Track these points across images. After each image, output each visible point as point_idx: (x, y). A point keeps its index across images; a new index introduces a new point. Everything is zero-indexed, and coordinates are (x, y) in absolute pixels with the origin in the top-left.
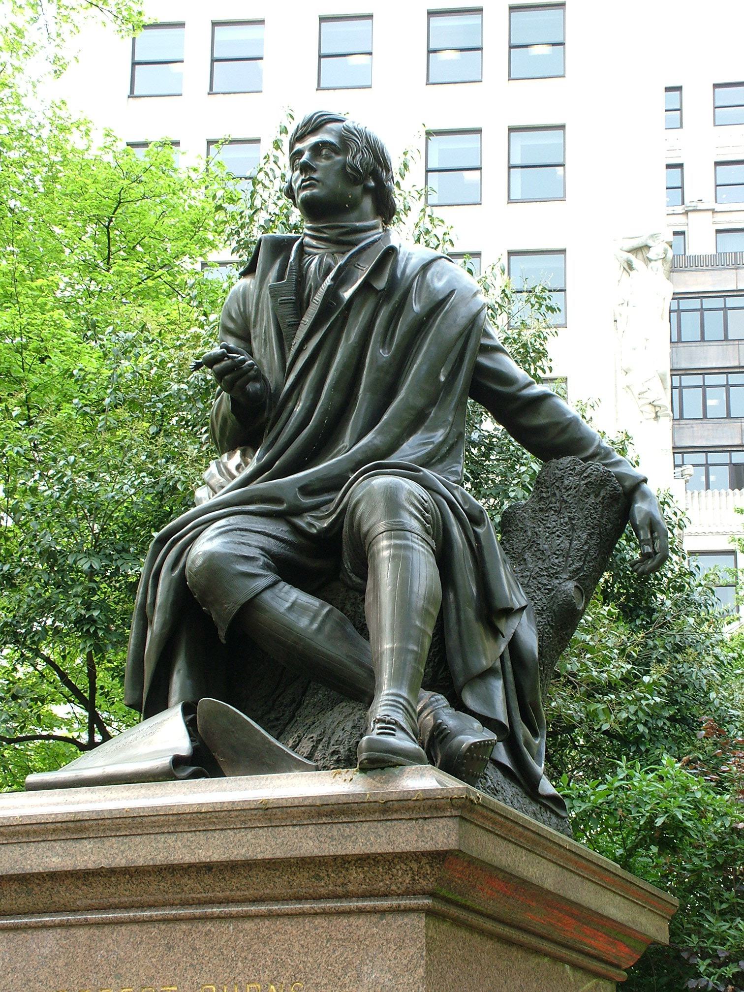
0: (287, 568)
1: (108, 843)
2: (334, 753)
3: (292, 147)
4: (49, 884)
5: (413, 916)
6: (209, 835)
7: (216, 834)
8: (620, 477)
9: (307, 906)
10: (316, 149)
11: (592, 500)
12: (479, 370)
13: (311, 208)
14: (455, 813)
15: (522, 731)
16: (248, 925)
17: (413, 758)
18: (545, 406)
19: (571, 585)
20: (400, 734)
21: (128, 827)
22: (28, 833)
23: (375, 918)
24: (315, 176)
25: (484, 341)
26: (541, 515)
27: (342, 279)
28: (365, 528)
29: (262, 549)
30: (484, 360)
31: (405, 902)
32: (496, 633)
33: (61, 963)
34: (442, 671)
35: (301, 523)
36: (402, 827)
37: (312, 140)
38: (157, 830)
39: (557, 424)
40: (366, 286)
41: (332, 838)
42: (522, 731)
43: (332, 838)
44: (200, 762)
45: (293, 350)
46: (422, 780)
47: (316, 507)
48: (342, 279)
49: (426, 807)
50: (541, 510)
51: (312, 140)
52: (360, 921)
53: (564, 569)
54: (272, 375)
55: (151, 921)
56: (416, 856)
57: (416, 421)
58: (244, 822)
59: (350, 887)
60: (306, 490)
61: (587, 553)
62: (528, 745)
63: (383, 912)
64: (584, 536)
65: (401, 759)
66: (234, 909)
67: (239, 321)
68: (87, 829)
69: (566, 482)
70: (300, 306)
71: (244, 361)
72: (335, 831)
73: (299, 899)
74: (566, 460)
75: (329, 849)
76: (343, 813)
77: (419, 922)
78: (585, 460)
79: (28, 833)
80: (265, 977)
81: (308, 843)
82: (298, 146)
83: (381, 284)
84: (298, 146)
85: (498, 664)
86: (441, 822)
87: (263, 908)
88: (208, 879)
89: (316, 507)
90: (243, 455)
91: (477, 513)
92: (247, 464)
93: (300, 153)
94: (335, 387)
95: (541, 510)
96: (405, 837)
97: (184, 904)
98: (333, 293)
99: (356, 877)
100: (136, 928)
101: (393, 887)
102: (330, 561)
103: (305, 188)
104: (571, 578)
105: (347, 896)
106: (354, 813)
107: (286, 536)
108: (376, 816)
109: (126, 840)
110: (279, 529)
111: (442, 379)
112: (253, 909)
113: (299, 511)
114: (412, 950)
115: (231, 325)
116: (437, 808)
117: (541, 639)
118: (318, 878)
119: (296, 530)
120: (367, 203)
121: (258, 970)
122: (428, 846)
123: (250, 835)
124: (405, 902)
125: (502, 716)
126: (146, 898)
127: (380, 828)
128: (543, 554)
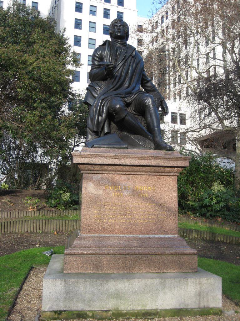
9: (156, 174)
16: (144, 176)
36: (179, 162)
52: (166, 177)
66: (142, 173)
72: (167, 162)
76: (169, 159)
79: (105, 157)
80: (148, 185)
86: (186, 162)
87: (148, 174)
88: (139, 168)
106: (171, 159)
116: (186, 159)
118: (160, 169)
127: (175, 162)
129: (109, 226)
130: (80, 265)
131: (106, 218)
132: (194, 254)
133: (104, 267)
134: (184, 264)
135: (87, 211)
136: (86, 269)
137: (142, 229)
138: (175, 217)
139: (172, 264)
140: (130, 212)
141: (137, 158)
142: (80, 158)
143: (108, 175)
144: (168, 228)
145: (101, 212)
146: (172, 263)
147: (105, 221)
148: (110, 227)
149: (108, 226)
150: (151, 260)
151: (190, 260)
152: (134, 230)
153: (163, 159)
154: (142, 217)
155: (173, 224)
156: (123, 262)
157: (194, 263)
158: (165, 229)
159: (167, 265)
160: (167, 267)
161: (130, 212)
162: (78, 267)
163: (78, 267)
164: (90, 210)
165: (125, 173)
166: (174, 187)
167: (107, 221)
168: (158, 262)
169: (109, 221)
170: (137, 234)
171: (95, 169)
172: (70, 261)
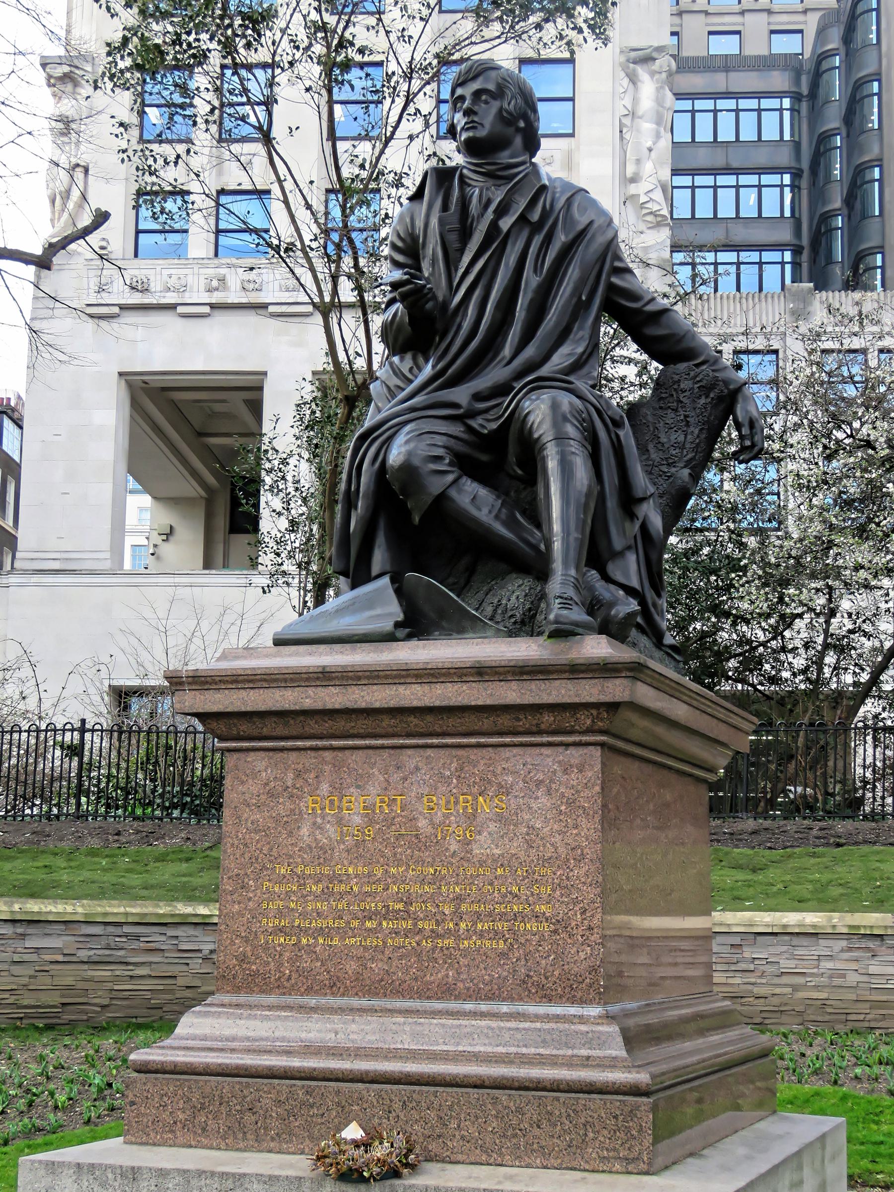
0: (466, 465)
1: (350, 689)
2: (512, 616)
3: (453, 92)
4: (302, 718)
5: (591, 748)
6: (433, 686)
7: (438, 686)
8: (726, 382)
9: (508, 740)
10: (477, 94)
11: (703, 401)
12: (612, 288)
13: (471, 147)
14: (629, 674)
15: (650, 594)
17: (588, 628)
18: (664, 319)
19: (686, 472)
20: (575, 607)
21: (368, 678)
22: (285, 680)
23: (561, 749)
24: (476, 119)
25: (617, 264)
26: (660, 412)
27: (502, 210)
28: (536, 436)
29: (444, 447)
30: (614, 280)
31: (585, 738)
32: (632, 516)
33: (312, 775)
34: (596, 555)
35: (474, 424)
37: (475, 86)
38: (390, 681)
39: (672, 335)
40: (523, 219)
41: (531, 691)
42: (650, 594)
43: (531, 691)
44: (415, 624)
45: (461, 271)
46: (597, 647)
47: (487, 411)
48: (502, 210)
49: (604, 669)
50: (661, 408)
51: (475, 86)
53: (680, 459)
54: (441, 294)
55: (383, 747)
56: (597, 706)
57: (562, 336)
58: (460, 677)
59: (543, 726)
60: (478, 397)
61: (698, 445)
62: (655, 605)
63: (567, 745)
64: (697, 431)
65: (580, 630)
67: (408, 240)
68: (334, 679)
69: (682, 386)
70: (465, 234)
71: (425, 286)
72: (533, 685)
73: (501, 734)
74: (682, 366)
75: (528, 699)
77: (597, 752)
78: (697, 365)
79: (285, 680)
80: (475, 790)
81: (510, 693)
82: (459, 91)
83: (535, 216)
84: (459, 91)
85: (633, 541)
86: (618, 682)
87: (473, 740)
88: (429, 718)
89: (487, 411)
90: (414, 359)
91: (618, 418)
92: (420, 370)
93: (462, 98)
94: (497, 307)
95: (661, 408)
96: (589, 691)
97: (409, 735)
98: (494, 226)
99: (548, 719)
100: (370, 752)
101: (577, 727)
102: (504, 457)
103: (468, 129)
104: (685, 467)
105: (540, 733)
107: (464, 436)
108: (566, 675)
109: (364, 688)
110: (456, 429)
111: (584, 298)
112: (465, 741)
113: (472, 414)
114: (590, 774)
115: (400, 244)
117: (663, 519)
118: (519, 720)
119: (470, 429)
120: (518, 141)
121: (469, 786)
122: (604, 698)
123: (465, 687)
124: (585, 738)
125: (635, 583)
126: (378, 730)
127: (570, 684)
128: (663, 445)
129: (319, 964)
130: (181, 1116)
131: (307, 930)
132: (636, 1091)
133: (265, 1129)
134: (591, 1135)
135: (239, 903)
136: (204, 1130)
137: (447, 976)
138: (590, 928)
139: (537, 1131)
140: (400, 906)
141: (408, 676)
142: (197, 693)
143: (321, 752)
144: (556, 973)
145: (292, 905)
146: (539, 1127)
147: (304, 941)
148: (323, 965)
149: (317, 960)
150: (451, 1108)
151: (616, 1117)
152: (416, 979)
153: (514, 674)
154: (451, 925)
155: (582, 955)
156: (340, 1109)
157: (634, 1132)
158: (547, 978)
159: (515, 1136)
160: (514, 1141)
161: (400, 906)
162: (175, 1123)
163: (175, 1123)
164: (250, 899)
165: (380, 742)
166: (587, 793)
167: (312, 941)
168: (477, 1117)
169: (321, 941)
170: (429, 998)
171: (265, 731)
172: (147, 1098)
